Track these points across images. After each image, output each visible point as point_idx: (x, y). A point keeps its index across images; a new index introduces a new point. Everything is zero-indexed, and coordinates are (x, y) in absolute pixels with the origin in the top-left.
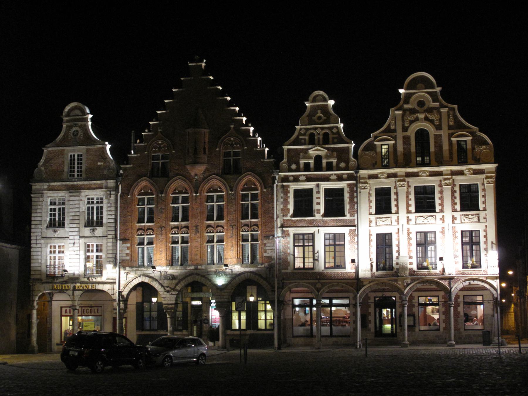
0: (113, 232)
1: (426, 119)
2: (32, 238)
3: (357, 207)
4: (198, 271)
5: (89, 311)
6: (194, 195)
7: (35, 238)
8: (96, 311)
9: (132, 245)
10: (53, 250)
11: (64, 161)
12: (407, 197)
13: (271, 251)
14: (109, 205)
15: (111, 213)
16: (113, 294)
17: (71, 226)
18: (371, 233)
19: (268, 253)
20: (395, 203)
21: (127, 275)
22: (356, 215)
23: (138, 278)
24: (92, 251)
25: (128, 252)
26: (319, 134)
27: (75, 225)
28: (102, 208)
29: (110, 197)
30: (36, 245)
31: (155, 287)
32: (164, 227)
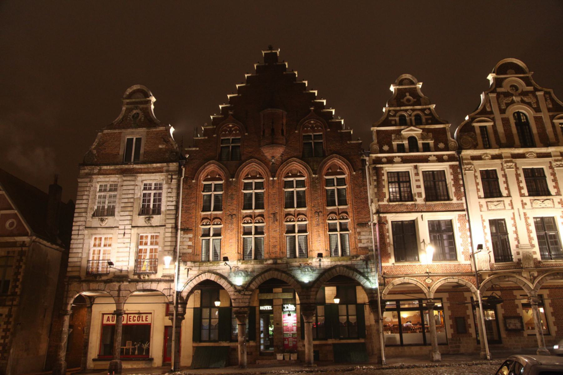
0: (173, 221)
1: (523, 102)
2: (74, 228)
3: (464, 189)
4: (277, 266)
5: (136, 319)
6: (271, 179)
7: (77, 228)
8: (144, 319)
9: (195, 236)
10: (98, 242)
11: (119, 145)
12: (518, 179)
13: (367, 240)
14: (170, 190)
15: (171, 199)
16: (170, 295)
17: (122, 213)
18: (484, 218)
19: (364, 243)
20: (505, 185)
21: (188, 271)
22: (464, 198)
23: (202, 275)
24: (146, 244)
25: (190, 243)
26: (410, 115)
27: (127, 213)
28: (160, 194)
29: (171, 181)
30: (77, 236)
31: (223, 286)
32: (234, 214)
